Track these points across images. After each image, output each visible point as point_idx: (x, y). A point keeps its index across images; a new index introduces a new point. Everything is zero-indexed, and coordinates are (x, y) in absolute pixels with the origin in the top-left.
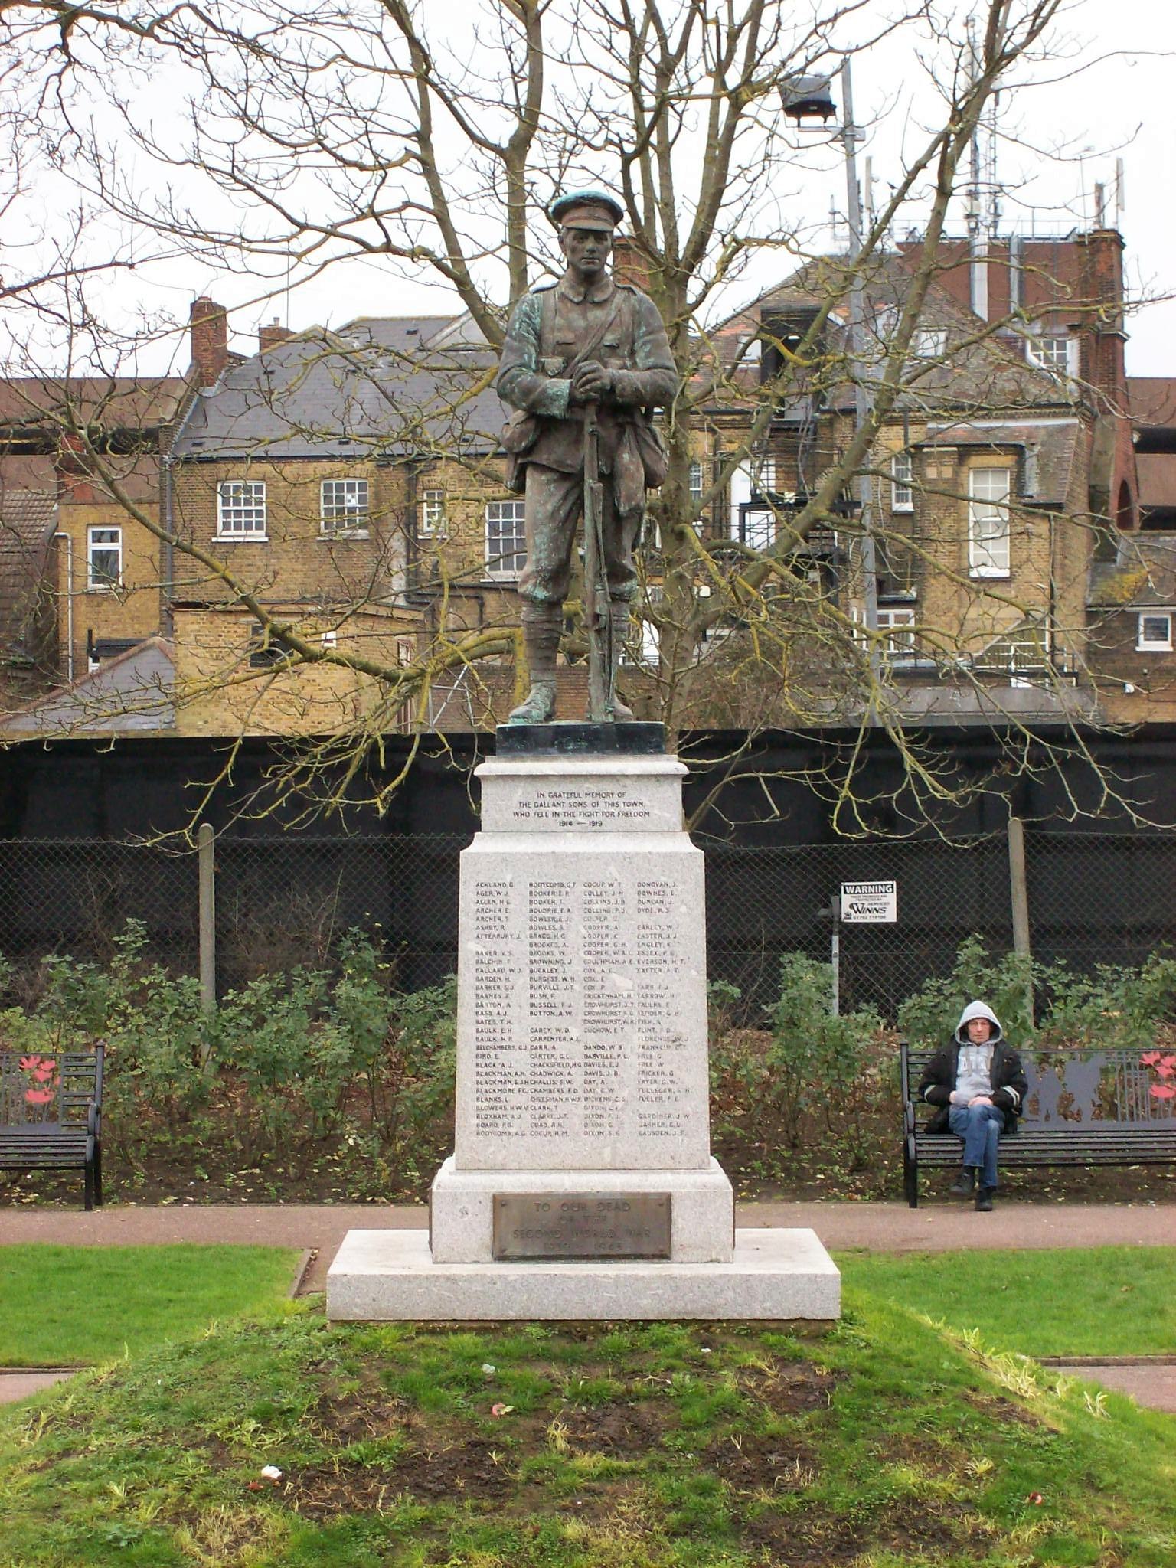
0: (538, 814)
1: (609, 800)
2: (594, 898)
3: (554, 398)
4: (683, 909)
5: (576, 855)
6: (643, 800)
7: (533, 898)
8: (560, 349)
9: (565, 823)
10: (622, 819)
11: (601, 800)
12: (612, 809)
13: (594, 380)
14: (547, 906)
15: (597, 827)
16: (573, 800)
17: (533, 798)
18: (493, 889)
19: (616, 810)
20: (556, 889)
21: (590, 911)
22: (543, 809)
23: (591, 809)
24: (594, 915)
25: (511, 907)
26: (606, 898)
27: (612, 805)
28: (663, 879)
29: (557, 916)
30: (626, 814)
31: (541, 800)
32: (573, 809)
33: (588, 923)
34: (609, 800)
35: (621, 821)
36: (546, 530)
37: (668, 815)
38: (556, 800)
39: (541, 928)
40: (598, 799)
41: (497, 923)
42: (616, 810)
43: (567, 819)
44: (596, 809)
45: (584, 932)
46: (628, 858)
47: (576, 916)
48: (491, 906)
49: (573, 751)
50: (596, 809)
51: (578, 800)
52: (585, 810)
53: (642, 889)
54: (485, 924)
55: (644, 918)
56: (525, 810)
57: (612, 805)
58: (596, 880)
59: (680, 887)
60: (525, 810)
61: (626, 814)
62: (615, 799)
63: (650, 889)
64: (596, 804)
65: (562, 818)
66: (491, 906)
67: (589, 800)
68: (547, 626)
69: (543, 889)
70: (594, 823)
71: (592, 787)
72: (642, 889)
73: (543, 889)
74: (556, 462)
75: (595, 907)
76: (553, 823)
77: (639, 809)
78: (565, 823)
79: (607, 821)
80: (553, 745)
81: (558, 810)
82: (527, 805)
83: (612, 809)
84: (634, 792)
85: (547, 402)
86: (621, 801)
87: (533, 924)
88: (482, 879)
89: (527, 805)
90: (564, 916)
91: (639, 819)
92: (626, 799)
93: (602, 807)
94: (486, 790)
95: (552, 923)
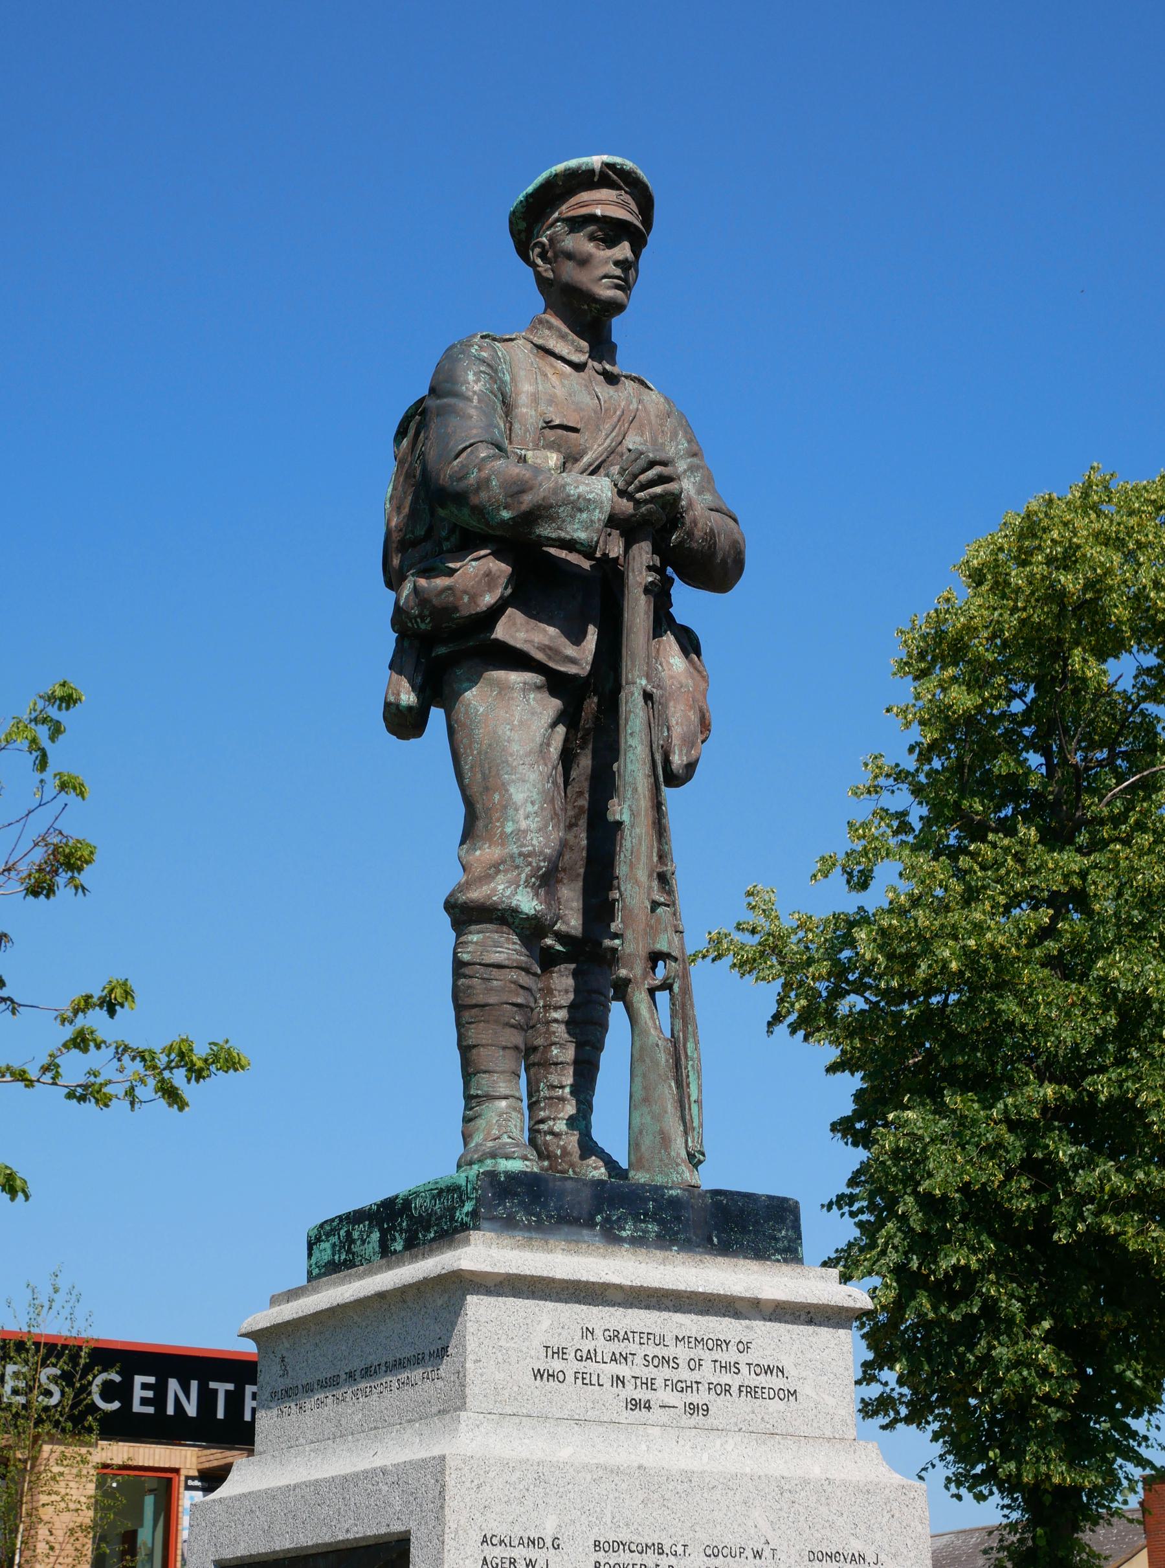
0: (582, 1378)
3: (578, 505)
5: (687, 1476)
6: (786, 1362)
8: (551, 435)
9: (635, 1404)
10: (744, 1404)
11: (707, 1356)
12: (726, 1378)
15: (698, 1419)
16: (651, 1350)
17: (572, 1340)
19: (734, 1381)
22: (590, 1366)
23: (684, 1374)
27: (725, 1367)
28: (856, 1546)
30: (752, 1392)
31: (587, 1345)
32: (650, 1372)
36: (533, 776)
37: (831, 1401)
38: (618, 1347)
40: (700, 1352)
42: (734, 1381)
43: (642, 1394)
44: (696, 1376)
46: (783, 1488)
50: (696, 1376)
51: (660, 1351)
52: (675, 1376)
56: (556, 1365)
57: (725, 1367)
60: (556, 1365)
61: (752, 1392)
62: (730, 1355)
64: (695, 1364)
65: (630, 1392)
67: (683, 1353)
68: (525, 979)
70: (693, 1408)
74: (543, 648)
76: (612, 1399)
77: (775, 1382)
78: (635, 1404)
79: (718, 1404)
80: (590, 1224)
81: (622, 1370)
82: (560, 1353)
83: (726, 1378)
84: (770, 1341)
85: (563, 511)
86: (743, 1359)
89: (560, 1353)
91: (776, 1405)
92: (753, 1356)
93: (707, 1374)
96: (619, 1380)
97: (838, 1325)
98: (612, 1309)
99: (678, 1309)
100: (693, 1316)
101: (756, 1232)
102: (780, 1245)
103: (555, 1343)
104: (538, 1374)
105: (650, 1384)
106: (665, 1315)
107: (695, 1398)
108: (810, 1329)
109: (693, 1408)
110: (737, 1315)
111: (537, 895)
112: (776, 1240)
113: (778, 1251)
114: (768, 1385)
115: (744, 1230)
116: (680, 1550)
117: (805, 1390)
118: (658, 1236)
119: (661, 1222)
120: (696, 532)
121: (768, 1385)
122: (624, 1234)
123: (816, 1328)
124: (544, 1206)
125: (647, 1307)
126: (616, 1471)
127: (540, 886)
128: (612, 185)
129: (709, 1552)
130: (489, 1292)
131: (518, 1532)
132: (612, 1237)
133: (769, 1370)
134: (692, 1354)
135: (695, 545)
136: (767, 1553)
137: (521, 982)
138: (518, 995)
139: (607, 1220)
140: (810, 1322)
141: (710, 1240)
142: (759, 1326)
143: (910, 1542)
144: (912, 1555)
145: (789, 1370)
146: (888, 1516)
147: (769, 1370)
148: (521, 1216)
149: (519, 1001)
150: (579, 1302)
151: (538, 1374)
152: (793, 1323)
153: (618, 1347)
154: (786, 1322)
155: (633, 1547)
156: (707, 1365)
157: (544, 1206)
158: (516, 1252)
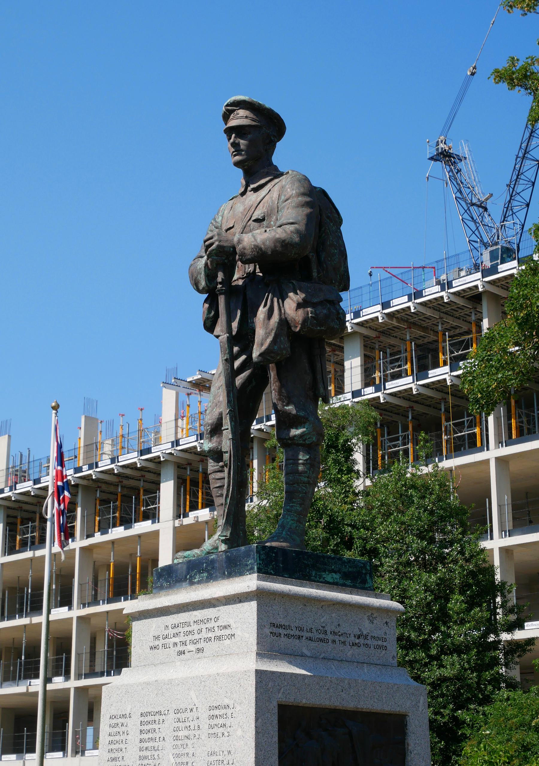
1: (209, 625)
2: (180, 724)
4: (239, 733)
5: (170, 682)
6: (231, 622)
7: (143, 728)
11: (204, 626)
12: (210, 635)
13: (212, 244)
14: (150, 735)
15: (200, 654)
16: (187, 629)
18: (120, 721)
20: (157, 718)
21: (177, 738)
23: (197, 636)
24: (179, 743)
25: (129, 737)
26: (187, 724)
28: (226, 701)
29: (156, 744)
30: (219, 638)
31: (166, 632)
33: (177, 751)
34: (209, 625)
35: (214, 645)
37: (247, 635)
38: (176, 631)
39: (146, 758)
41: (120, 755)
43: (182, 648)
45: (172, 760)
47: (169, 743)
48: (117, 738)
49: (199, 582)
53: (212, 713)
54: (113, 756)
55: (212, 744)
56: (157, 643)
58: (183, 706)
59: (238, 708)
60: (157, 643)
61: (219, 638)
63: (217, 712)
66: (117, 738)
67: (195, 627)
69: (150, 718)
70: (199, 650)
71: (198, 614)
72: (212, 713)
73: (150, 718)
75: (181, 734)
77: (227, 632)
80: (186, 579)
81: (177, 640)
82: (157, 638)
83: (210, 635)
87: (141, 754)
88: (114, 713)
90: (161, 744)
91: (227, 642)
92: (220, 623)
93: (204, 635)
94: (137, 627)
95: (154, 752)
96: (175, 644)
97: (251, 600)
98: (174, 616)
99: (203, 608)
100: (200, 611)
101: (240, 564)
102: (249, 568)
103: (156, 634)
104: (151, 648)
105: (184, 643)
106: (191, 613)
107: (199, 646)
108: (241, 604)
109: (199, 650)
110: (214, 606)
111: (210, 441)
112: (247, 565)
113: (248, 571)
114: (226, 634)
115: (236, 565)
116: (166, 712)
117: (238, 633)
118: (207, 577)
119: (208, 571)
120: (246, 251)
121: (226, 634)
122: (196, 580)
123: (242, 604)
124: (172, 577)
125: (185, 612)
126: (148, 684)
127: (211, 436)
128: (233, 111)
129: (176, 712)
130: (138, 619)
131: (120, 713)
132: (192, 583)
133: (225, 627)
134: (199, 627)
135: (249, 257)
136: (194, 710)
137: (217, 477)
138: (216, 483)
139: (191, 577)
140: (240, 602)
141: (224, 573)
142: (222, 608)
143: (246, 697)
144: (247, 702)
145: (233, 625)
146: (239, 686)
147: (225, 627)
148: (165, 584)
149: (218, 485)
150: (164, 616)
151: (151, 648)
152: (234, 604)
153: (176, 631)
154: (232, 604)
155: (152, 714)
156: (204, 630)
157: (172, 577)
158: (151, 601)
